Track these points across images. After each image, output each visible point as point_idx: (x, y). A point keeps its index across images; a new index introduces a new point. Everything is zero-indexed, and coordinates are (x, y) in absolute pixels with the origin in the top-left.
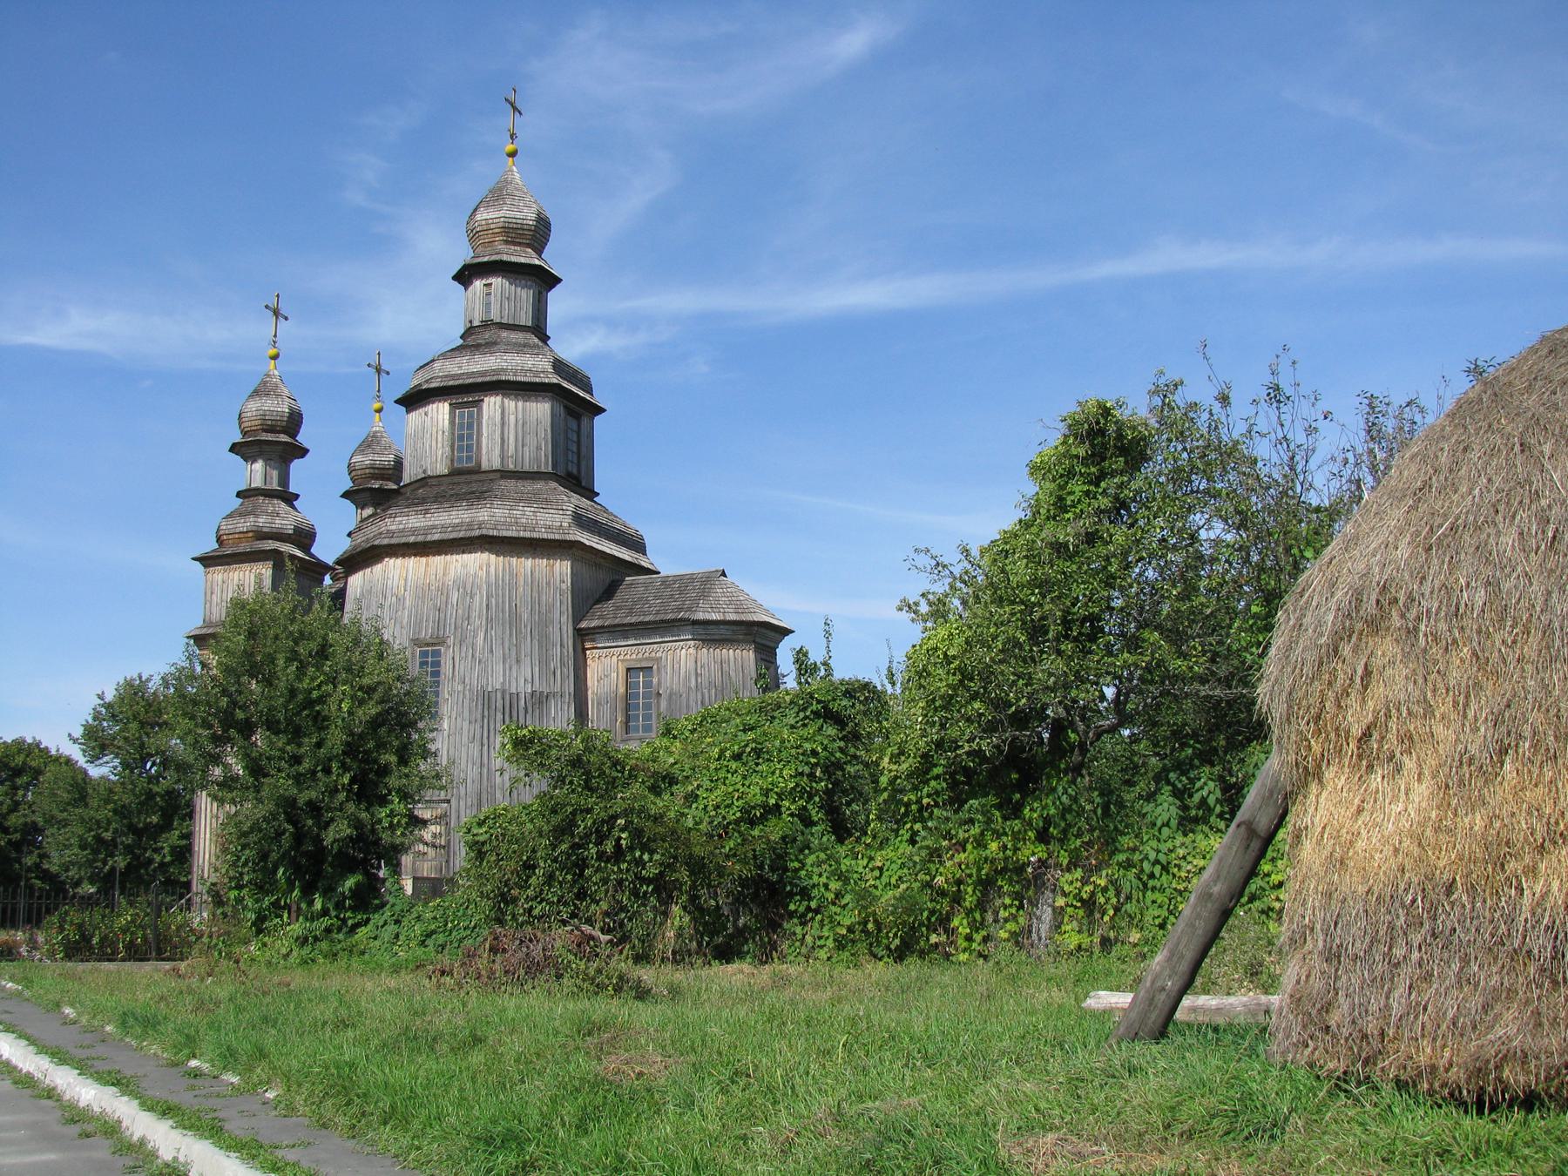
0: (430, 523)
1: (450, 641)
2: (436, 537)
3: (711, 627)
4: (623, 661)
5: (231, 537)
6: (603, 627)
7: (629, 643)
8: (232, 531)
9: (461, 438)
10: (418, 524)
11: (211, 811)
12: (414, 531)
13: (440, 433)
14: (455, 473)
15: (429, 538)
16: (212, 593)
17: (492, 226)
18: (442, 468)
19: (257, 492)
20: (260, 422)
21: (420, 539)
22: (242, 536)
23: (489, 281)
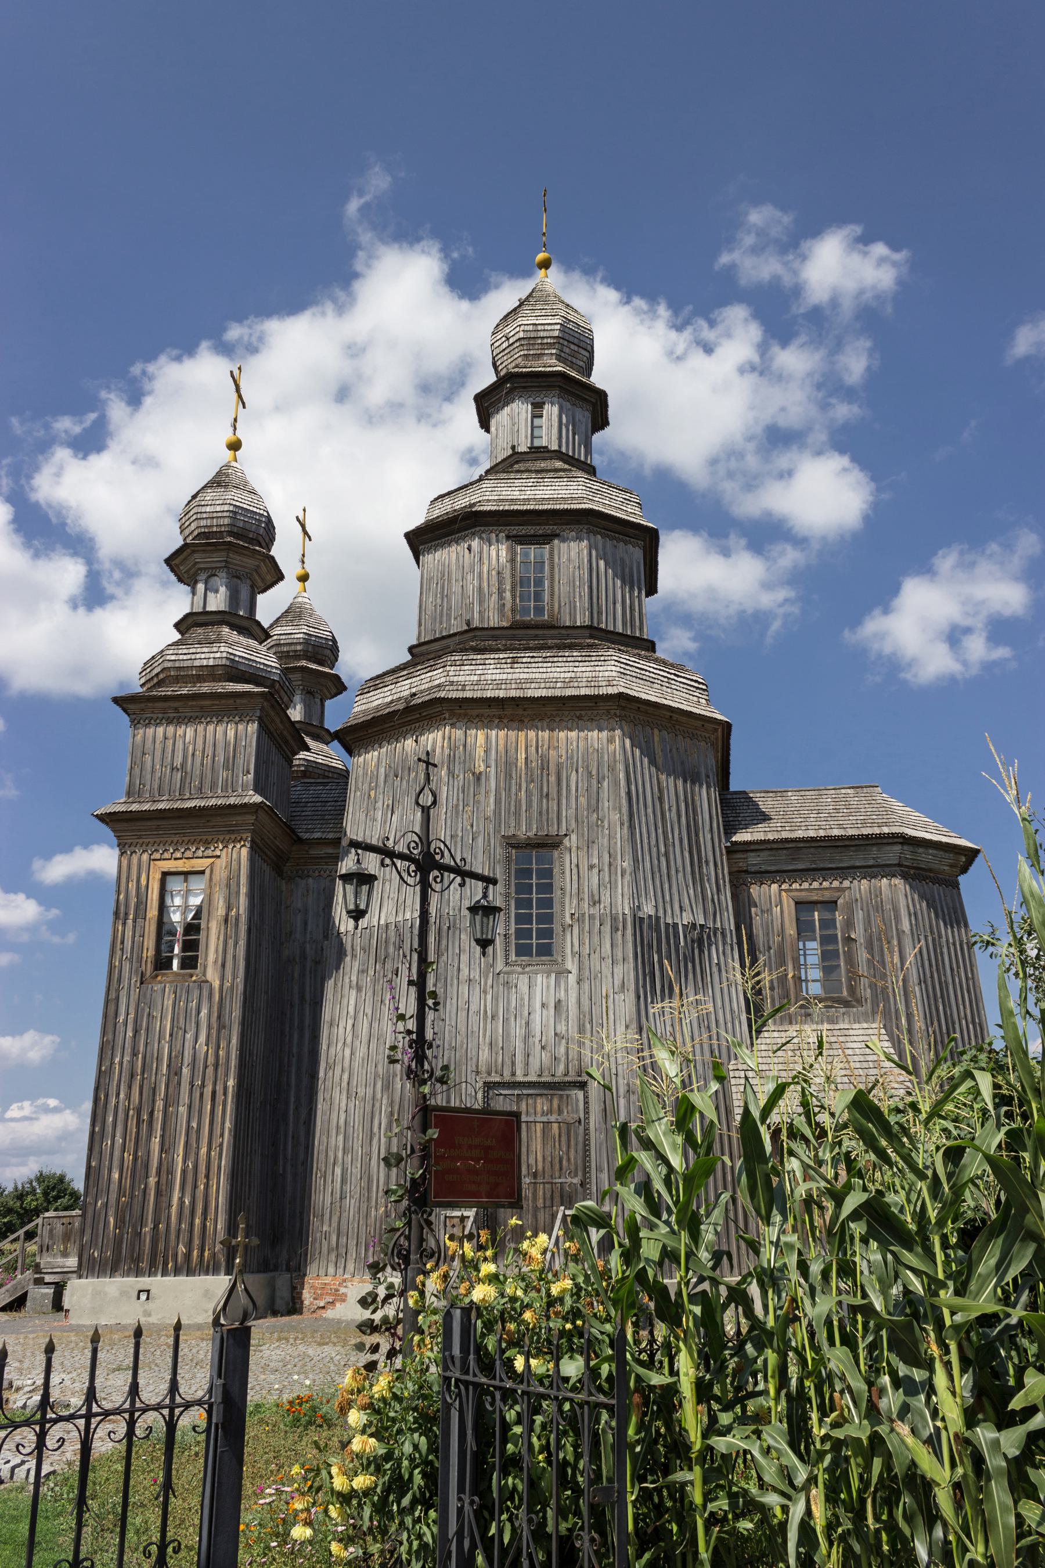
0: (525, 676)
1: (566, 841)
2: (544, 693)
3: (921, 850)
4: (785, 890)
6: (768, 841)
9: (524, 582)
10: (505, 676)
11: (129, 1097)
12: (499, 684)
13: (494, 573)
14: (515, 626)
15: (530, 693)
16: (144, 754)
17: (542, 334)
18: (494, 620)
19: (218, 617)
20: (226, 521)
21: (513, 694)
23: (538, 400)
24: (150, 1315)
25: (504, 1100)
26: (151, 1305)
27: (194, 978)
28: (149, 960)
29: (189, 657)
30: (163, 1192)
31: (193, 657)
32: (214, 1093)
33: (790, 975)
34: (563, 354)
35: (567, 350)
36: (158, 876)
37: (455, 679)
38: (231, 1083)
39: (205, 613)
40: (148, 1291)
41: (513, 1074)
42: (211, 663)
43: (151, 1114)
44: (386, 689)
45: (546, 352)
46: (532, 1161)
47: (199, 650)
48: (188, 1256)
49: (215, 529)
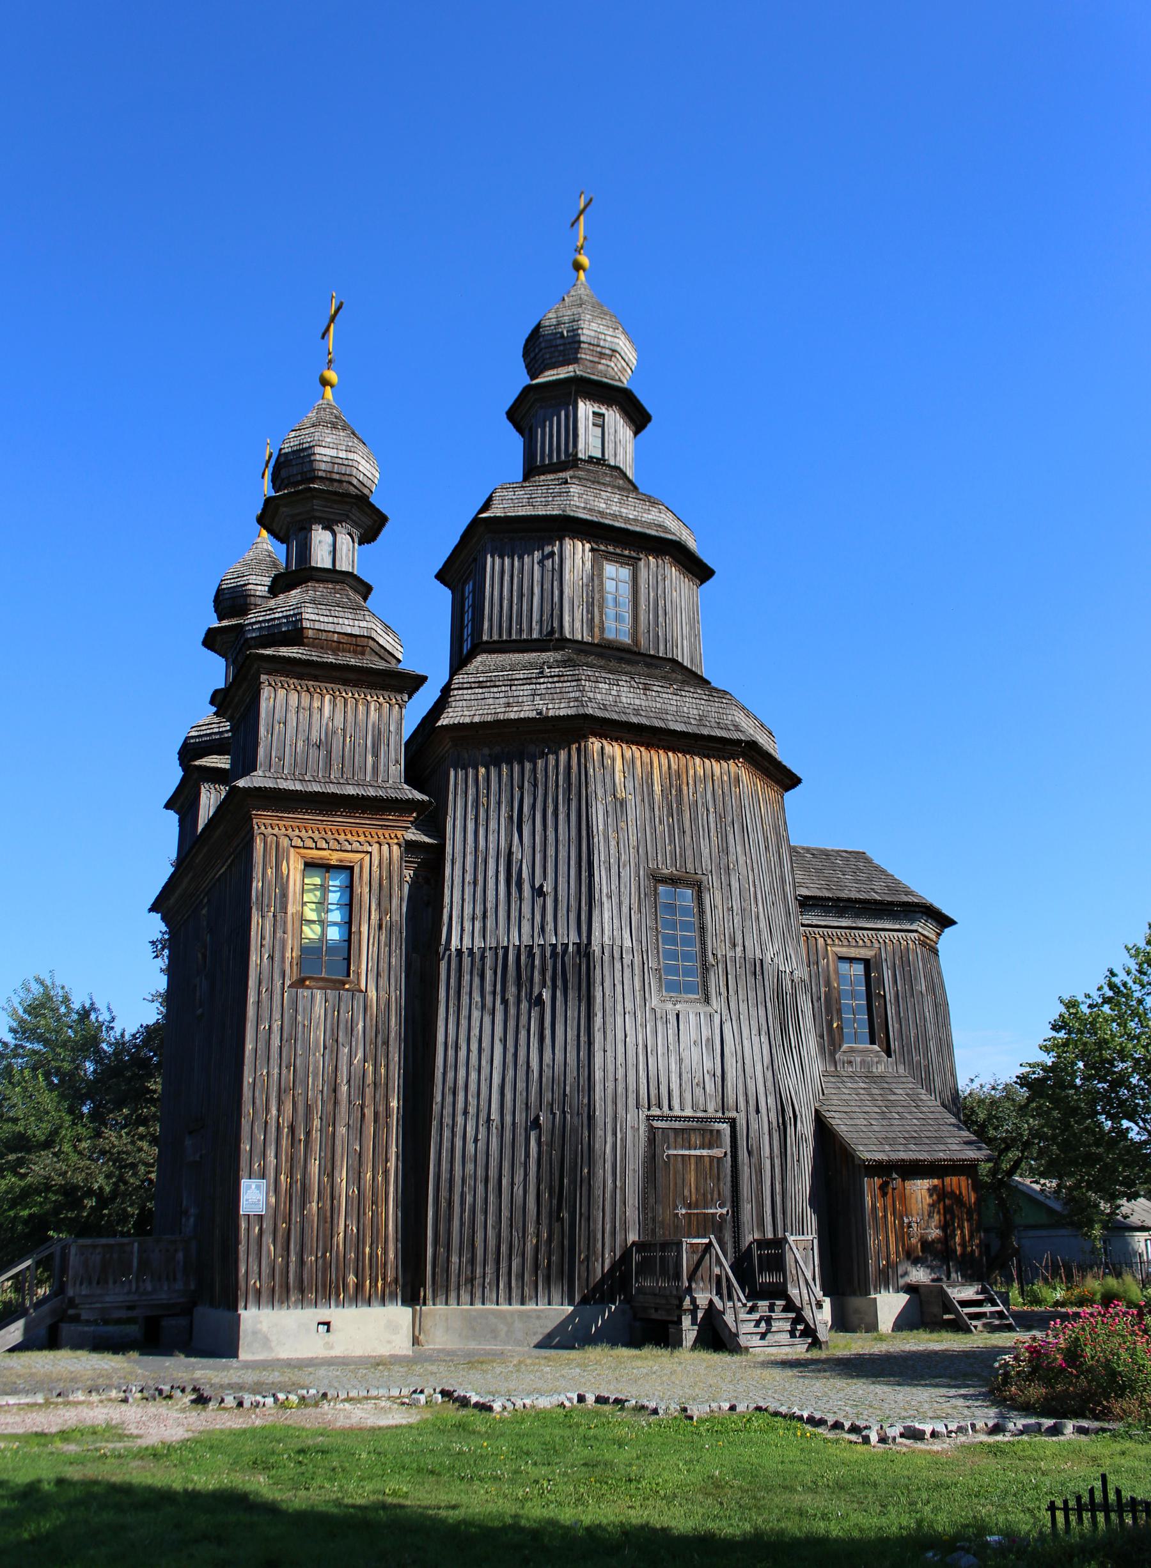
5: (324, 636)
7: (844, 924)
8: (330, 627)
22: (344, 639)
23: (597, 410)
24: (332, 1348)
25: (663, 1132)
26: (331, 1337)
27: (347, 986)
28: (295, 963)
29: (331, 619)
30: (328, 1218)
31: (336, 620)
32: (376, 1114)
33: (835, 1025)
34: (616, 369)
35: (619, 366)
36: (301, 866)
37: (591, 695)
38: (394, 1104)
39: (334, 571)
40: (328, 1324)
41: (670, 1109)
42: (356, 631)
43: (308, 1134)
44: (495, 690)
45: (603, 361)
46: (686, 1193)
47: (341, 614)
48: (359, 1287)
49: (337, 477)
